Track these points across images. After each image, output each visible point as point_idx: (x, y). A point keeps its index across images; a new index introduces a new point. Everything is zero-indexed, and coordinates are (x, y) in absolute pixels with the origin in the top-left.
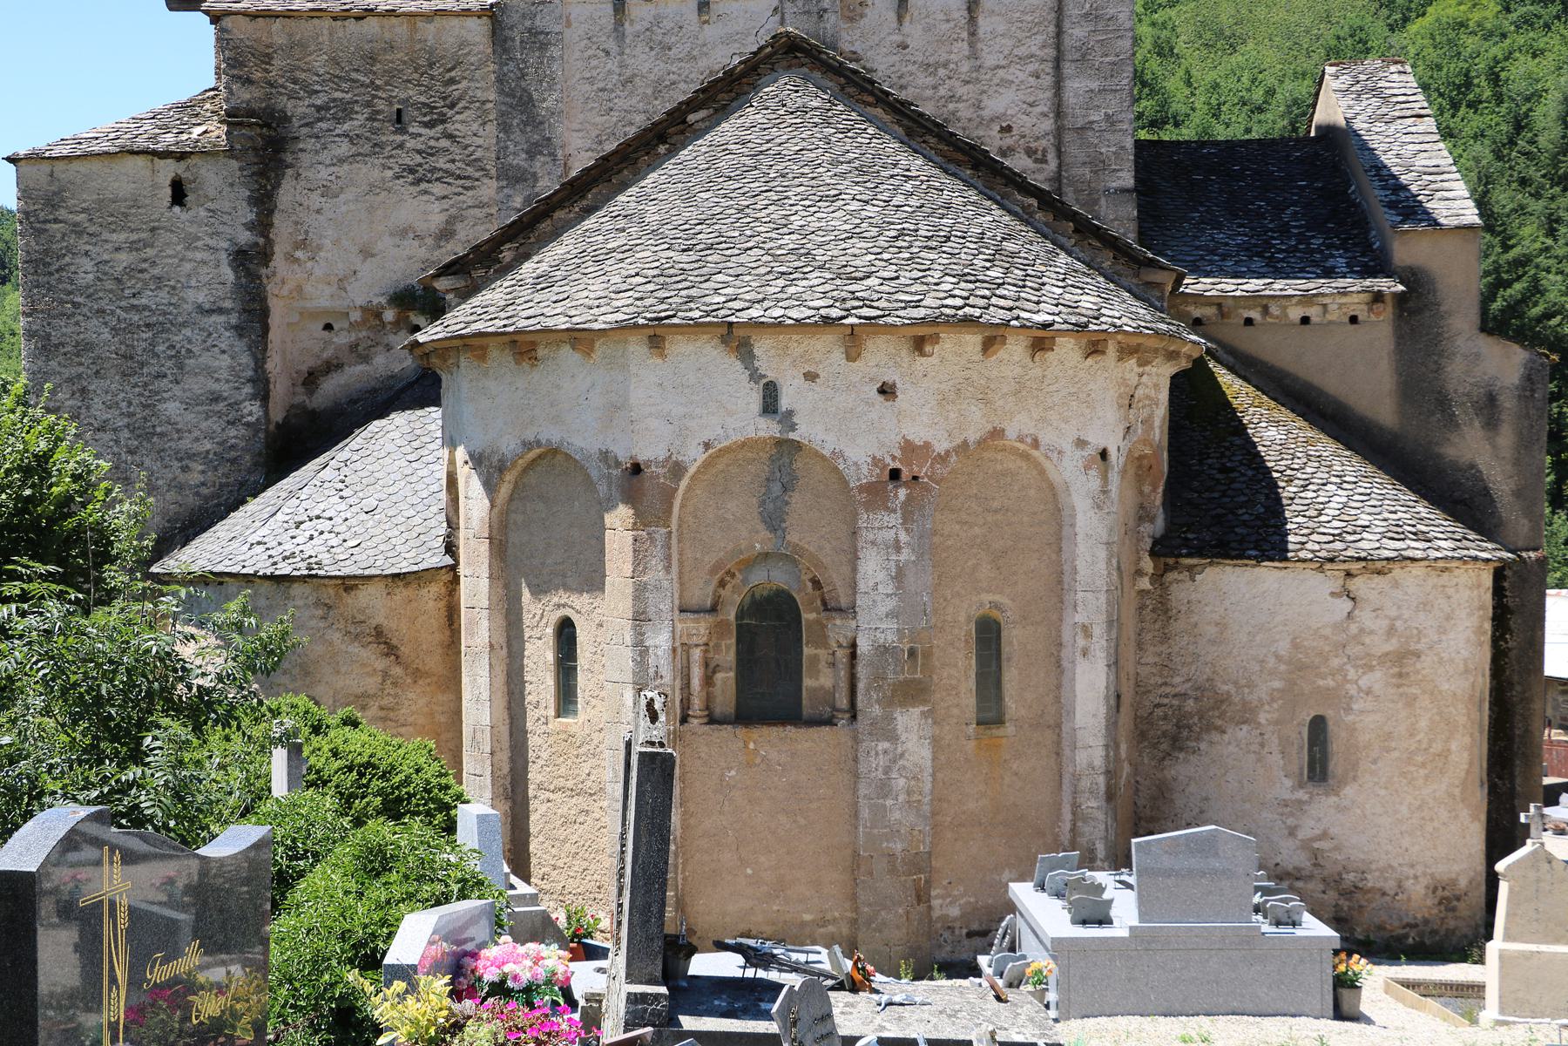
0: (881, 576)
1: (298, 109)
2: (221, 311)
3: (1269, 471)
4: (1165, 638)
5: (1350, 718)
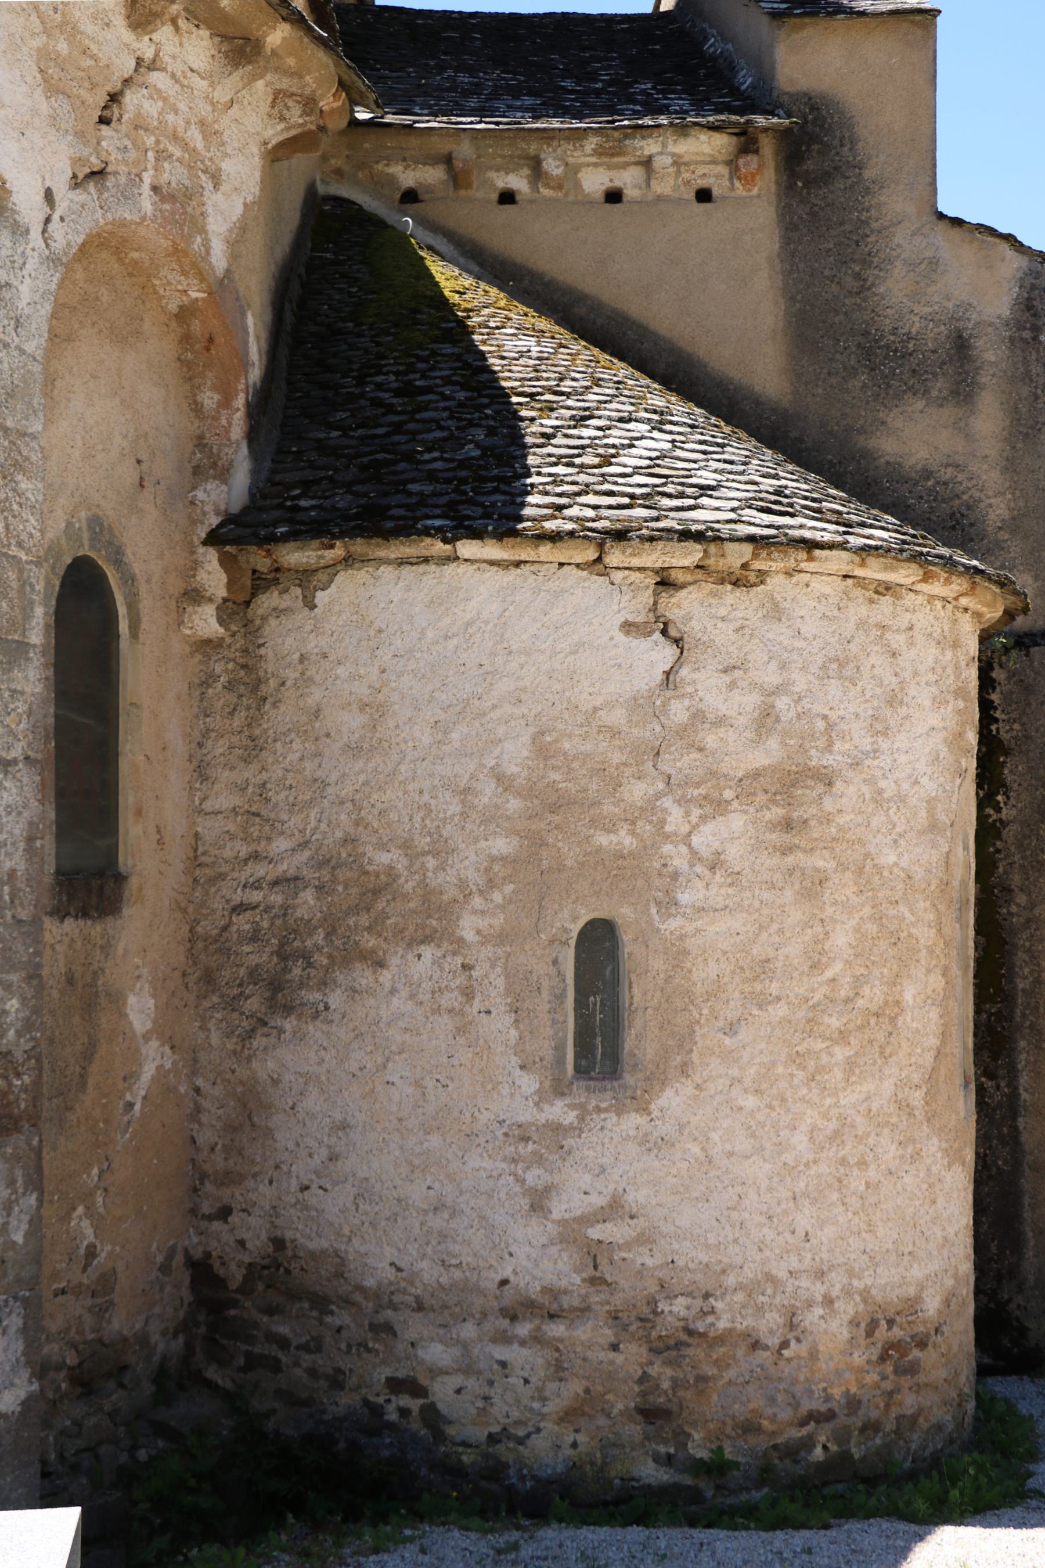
3: (504, 395)
4: (253, 748)
5: (674, 924)
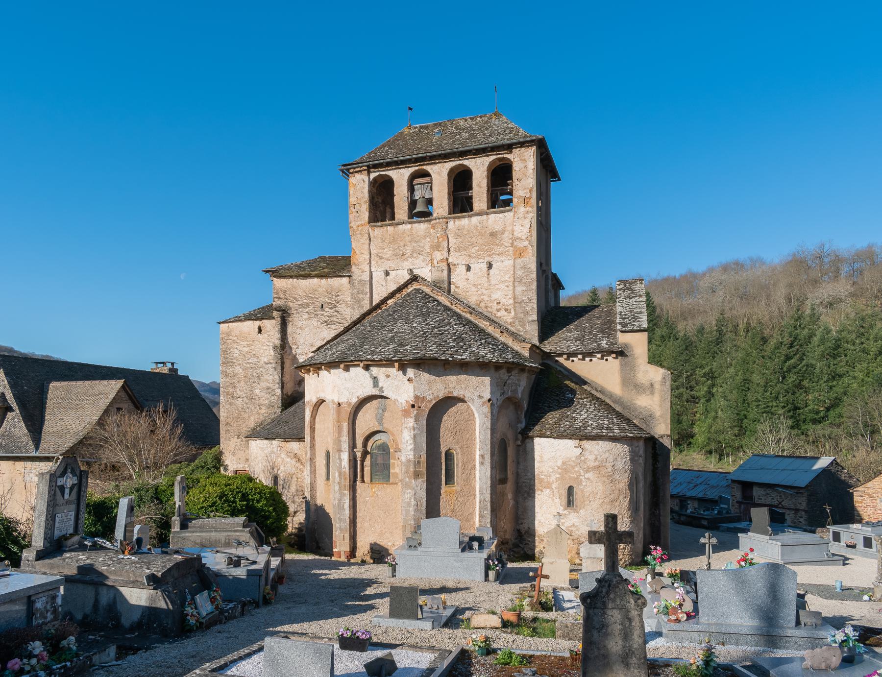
0: (409, 438)
2: (270, 363)
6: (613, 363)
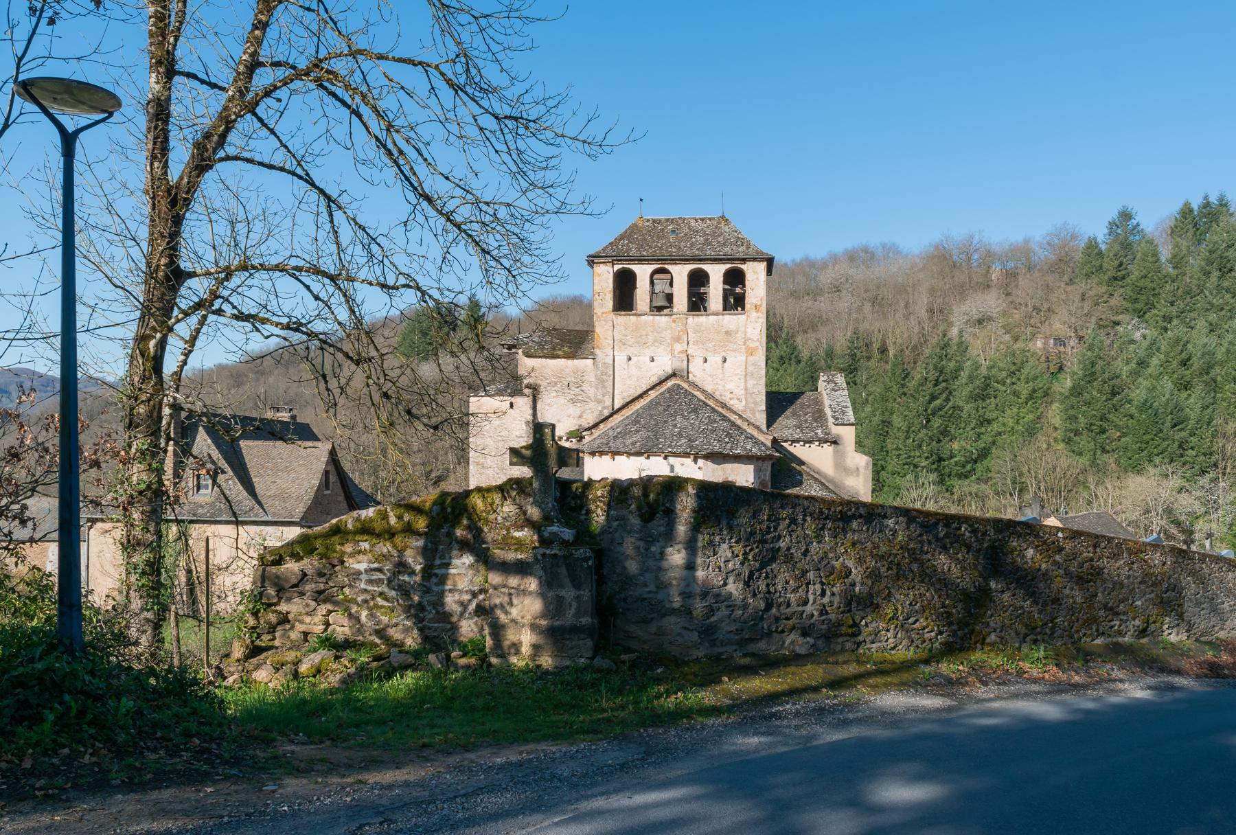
1: (543, 384)
6: (828, 449)
